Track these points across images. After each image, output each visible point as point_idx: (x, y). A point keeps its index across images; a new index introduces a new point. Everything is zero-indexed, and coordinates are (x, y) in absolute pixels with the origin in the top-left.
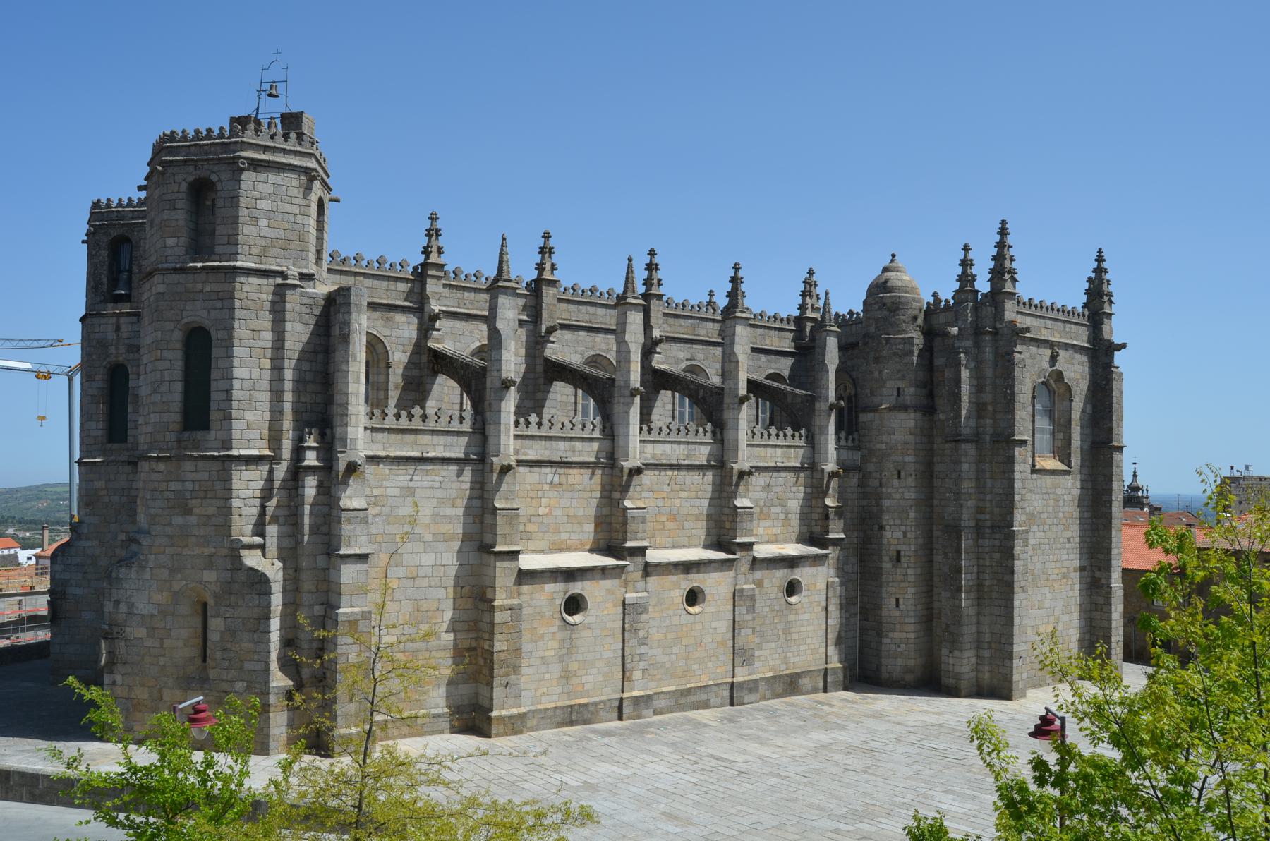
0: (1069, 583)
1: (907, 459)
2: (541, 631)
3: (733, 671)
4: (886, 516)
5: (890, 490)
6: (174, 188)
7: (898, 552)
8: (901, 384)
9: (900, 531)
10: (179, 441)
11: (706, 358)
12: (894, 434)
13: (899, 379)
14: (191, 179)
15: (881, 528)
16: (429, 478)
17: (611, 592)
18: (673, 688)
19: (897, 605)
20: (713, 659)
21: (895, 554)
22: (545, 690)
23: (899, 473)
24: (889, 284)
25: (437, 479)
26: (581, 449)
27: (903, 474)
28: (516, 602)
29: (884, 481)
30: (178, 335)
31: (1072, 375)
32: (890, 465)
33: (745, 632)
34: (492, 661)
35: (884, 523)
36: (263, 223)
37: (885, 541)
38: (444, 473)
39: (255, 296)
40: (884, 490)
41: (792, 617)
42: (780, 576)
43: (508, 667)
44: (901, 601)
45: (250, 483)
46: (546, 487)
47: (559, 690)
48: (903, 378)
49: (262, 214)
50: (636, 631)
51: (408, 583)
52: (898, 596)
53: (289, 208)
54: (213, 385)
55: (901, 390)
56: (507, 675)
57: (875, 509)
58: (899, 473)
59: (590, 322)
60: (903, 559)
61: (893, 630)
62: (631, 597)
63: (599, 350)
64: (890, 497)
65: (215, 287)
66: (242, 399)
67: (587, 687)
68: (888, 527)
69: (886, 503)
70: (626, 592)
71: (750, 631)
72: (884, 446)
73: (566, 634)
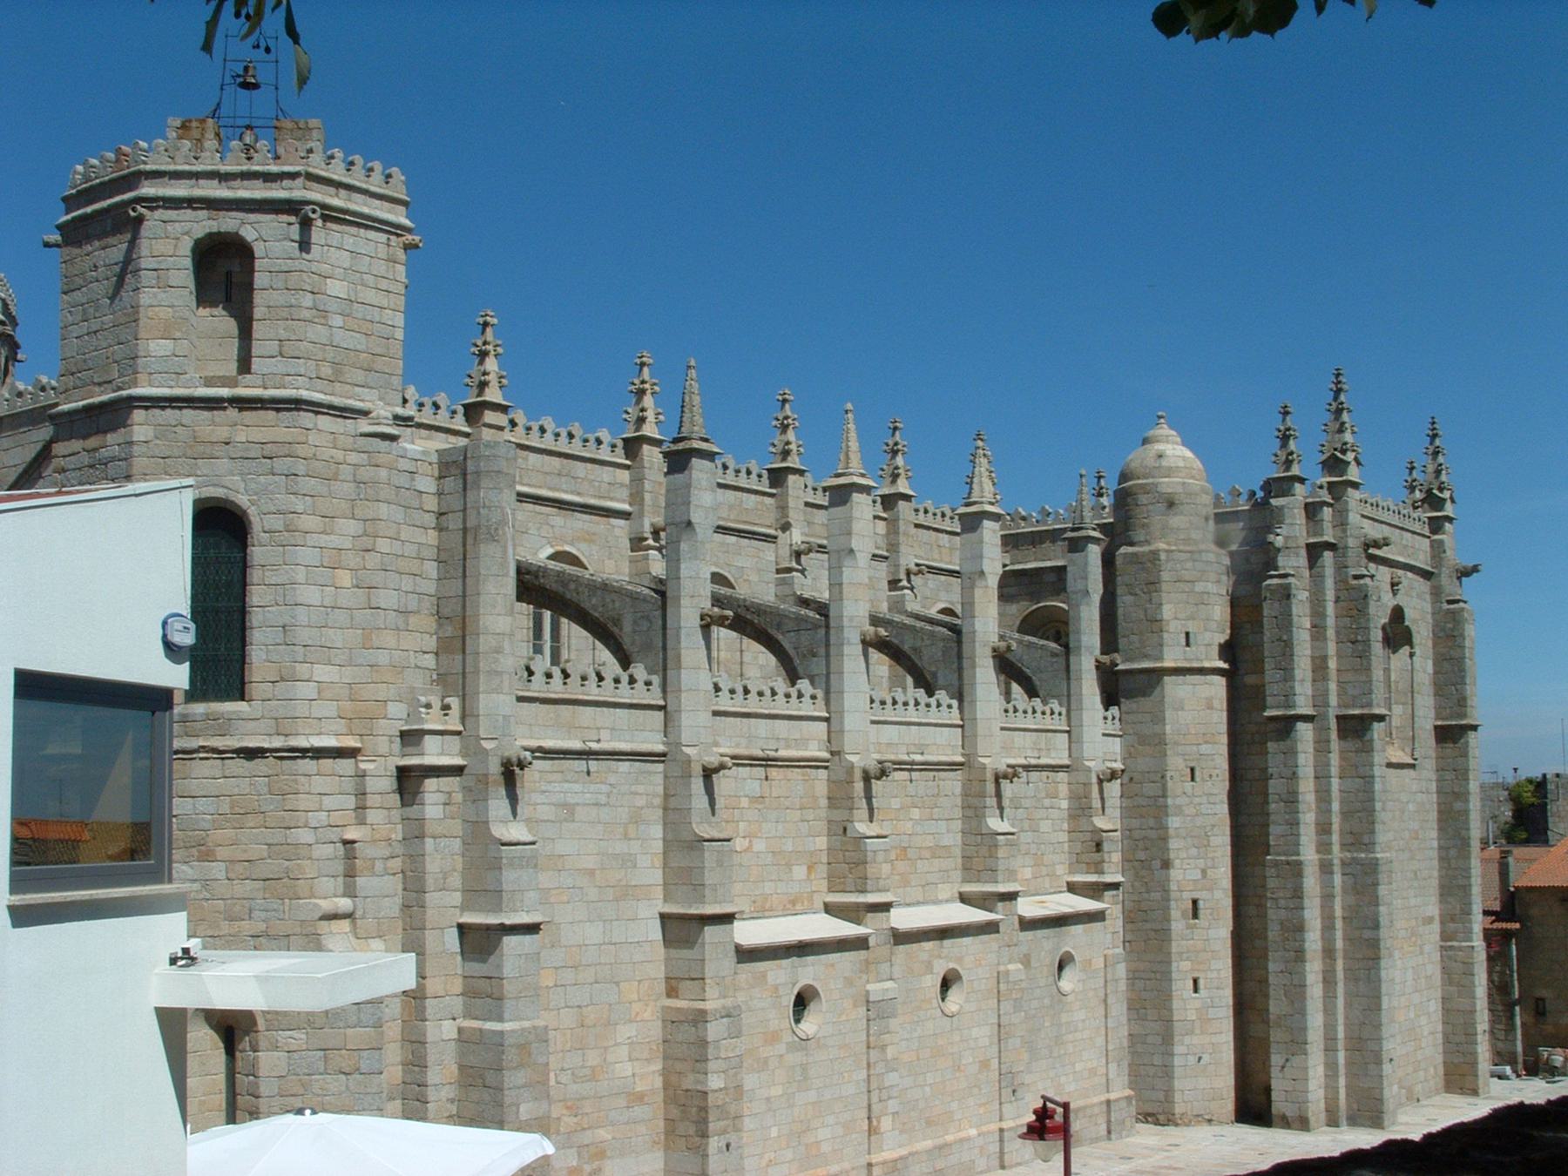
0: (1419, 942)
1: (1205, 749)
2: (765, 1052)
3: (1000, 1110)
4: (1173, 844)
5: (1178, 801)
7: (1195, 902)
9: (1196, 867)
12: (1183, 709)
13: (1188, 619)
14: (200, 234)
15: (1166, 865)
16: (593, 788)
17: (849, 982)
18: (929, 1144)
19: (1196, 990)
20: (975, 1091)
21: (1190, 906)
22: (772, 1155)
23: (1192, 770)
24: (1164, 463)
25: (605, 788)
26: (785, 736)
27: (1197, 773)
28: (729, 1002)
33: (1014, 1043)
34: (704, 1109)
35: (1172, 856)
36: (337, 321)
37: (1173, 887)
38: (612, 779)
39: (327, 453)
41: (1064, 1018)
42: (1047, 944)
43: (727, 1119)
44: (1201, 983)
45: (324, 797)
46: (745, 802)
47: (789, 1154)
49: (333, 306)
50: (883, 1048)
51: (568, 976)
52: (1196, 975)
53: (370, 296)
54: (256, 618)
55: (1191, 636)
56: (725, 1132)
57: (1153, 834)
58: (1192, 770)
60: (1201, 913)
61: (1191, 1032)
62: (875, 989)
64: (1179, 810)
65: (257, 435)
66: (310, 643)
67: (825, 1148)
68: (1177, 863)
69: (1174, 822)
70: (868, 982)
71: (1018, 1041)
73: (795, 1058)
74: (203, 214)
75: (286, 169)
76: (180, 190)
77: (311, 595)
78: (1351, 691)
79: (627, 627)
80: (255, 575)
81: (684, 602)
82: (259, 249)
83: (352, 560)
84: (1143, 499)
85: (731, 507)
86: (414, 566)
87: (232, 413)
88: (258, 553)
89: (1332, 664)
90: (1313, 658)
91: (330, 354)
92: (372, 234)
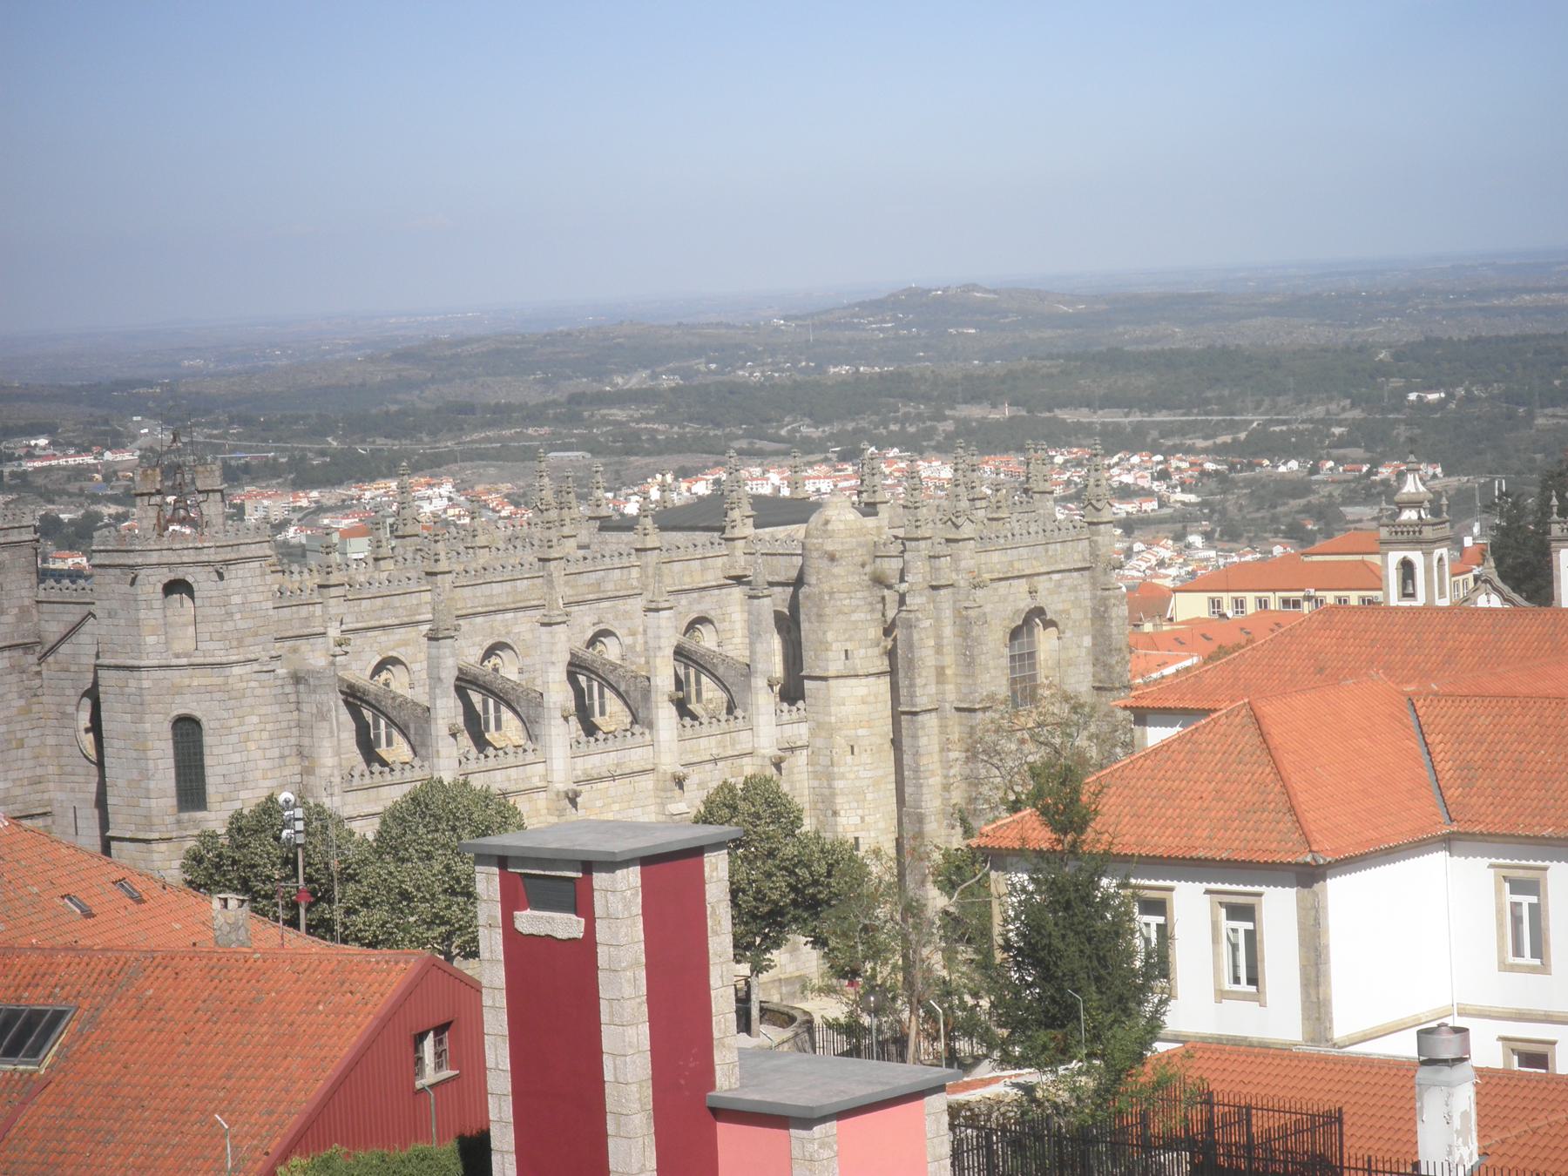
1: (861, 732)
4: (839, 800)
6: (149, 588)
8: (849, 646)
10: (179, 822)
11: (616, 618)
13: (846, 640)
15: (835, 813)
23: (852, 747)
24: (830, 527)
29: (835, 759)
30: (167, 726)
31: (1060, 607)
32: (840, 741)
40: (836, 769)
48: (850, 639)
53: (254, 597)
54: (208, 771)
57: (827, 792)
58: (852, 747)
59: (487, 606)
63: (499, 635)
64: (843, 777)
68: (842, 813)
72: (833, 719)
74: (166, 570)
75: (206, 544)
76: (154, 558)
77: (236, 758)
78: (964, 690)
79: (412, 731)
80: (206, 751)
81: (440, 722)
82: (195, 586)
83: (256, 735)
84: (815, 554)
85: (508, 594)
86: (287, 732)
87: (190, 671)
88: (208, 740)
89: (949, 672)
90: (937, 668)
91: (236, 635)
92: (252, 565)
